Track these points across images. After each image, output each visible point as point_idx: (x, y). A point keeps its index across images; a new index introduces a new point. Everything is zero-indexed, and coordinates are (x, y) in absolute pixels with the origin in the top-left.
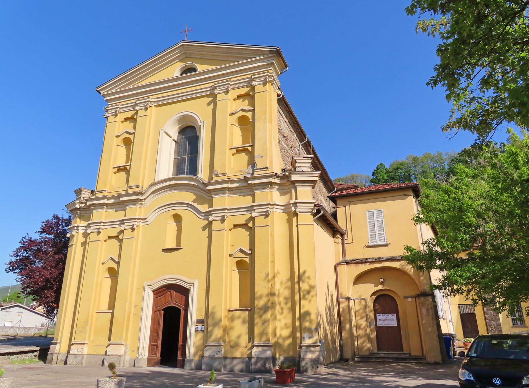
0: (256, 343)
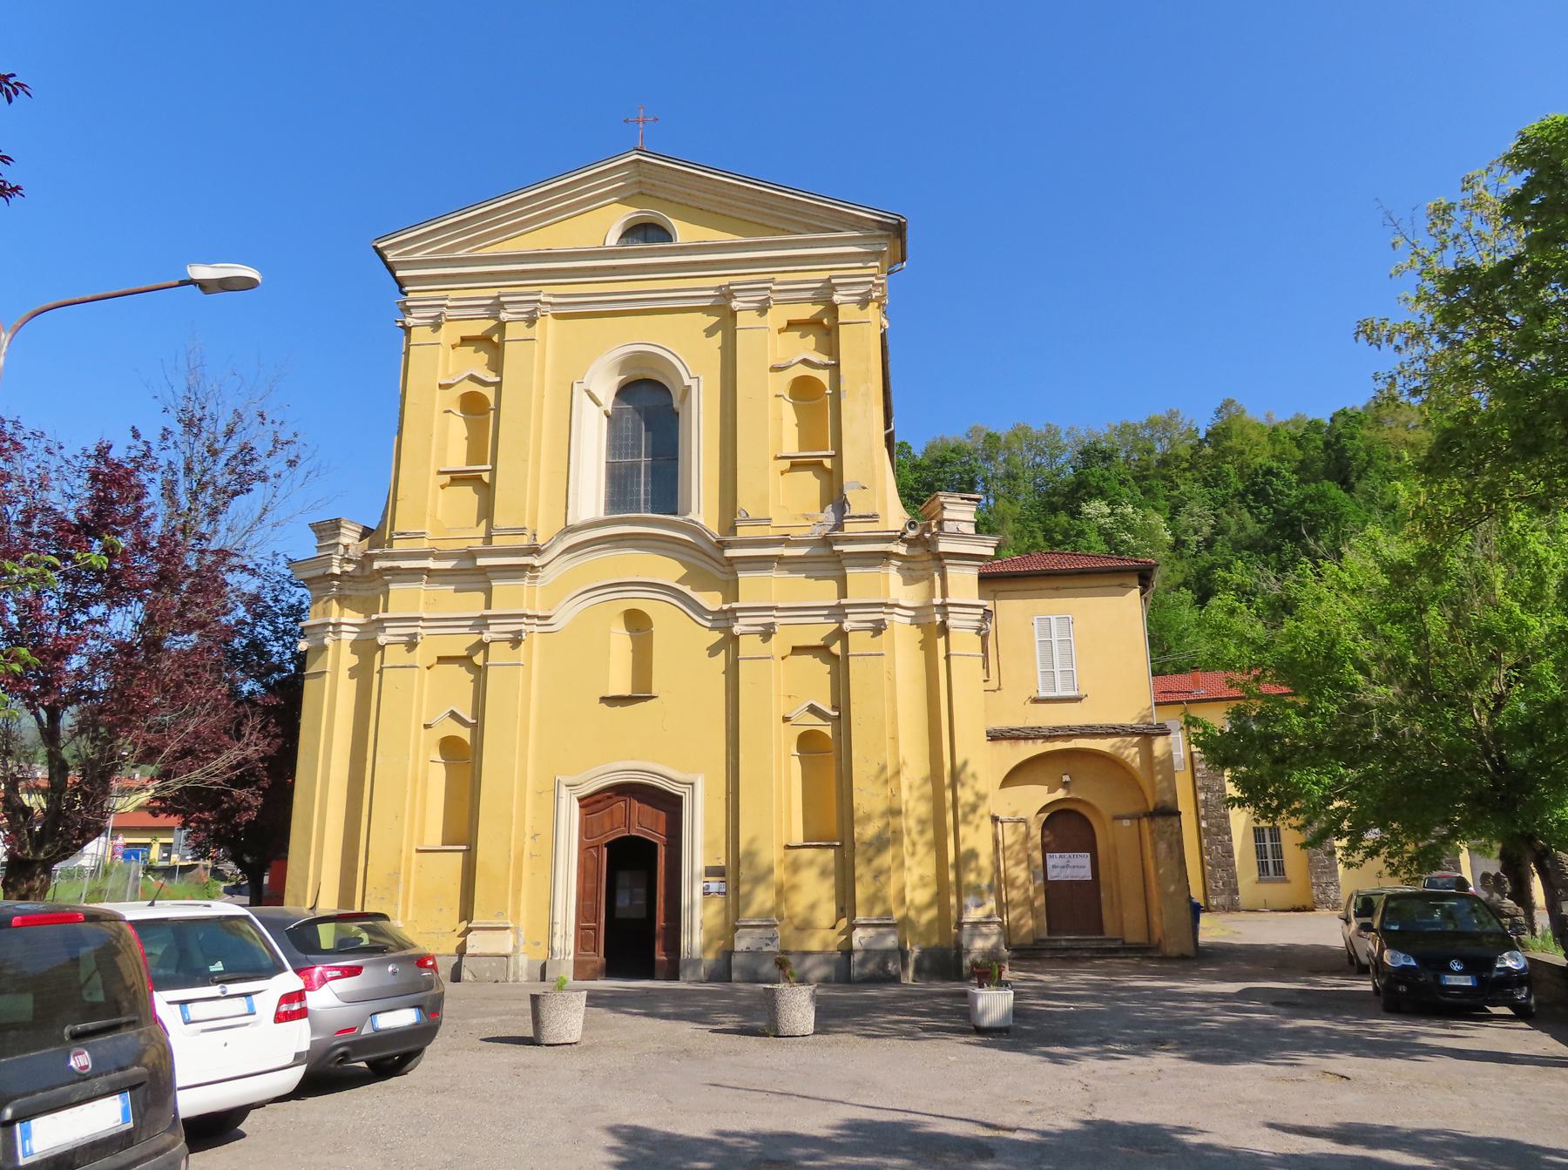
0: (860, 917)
